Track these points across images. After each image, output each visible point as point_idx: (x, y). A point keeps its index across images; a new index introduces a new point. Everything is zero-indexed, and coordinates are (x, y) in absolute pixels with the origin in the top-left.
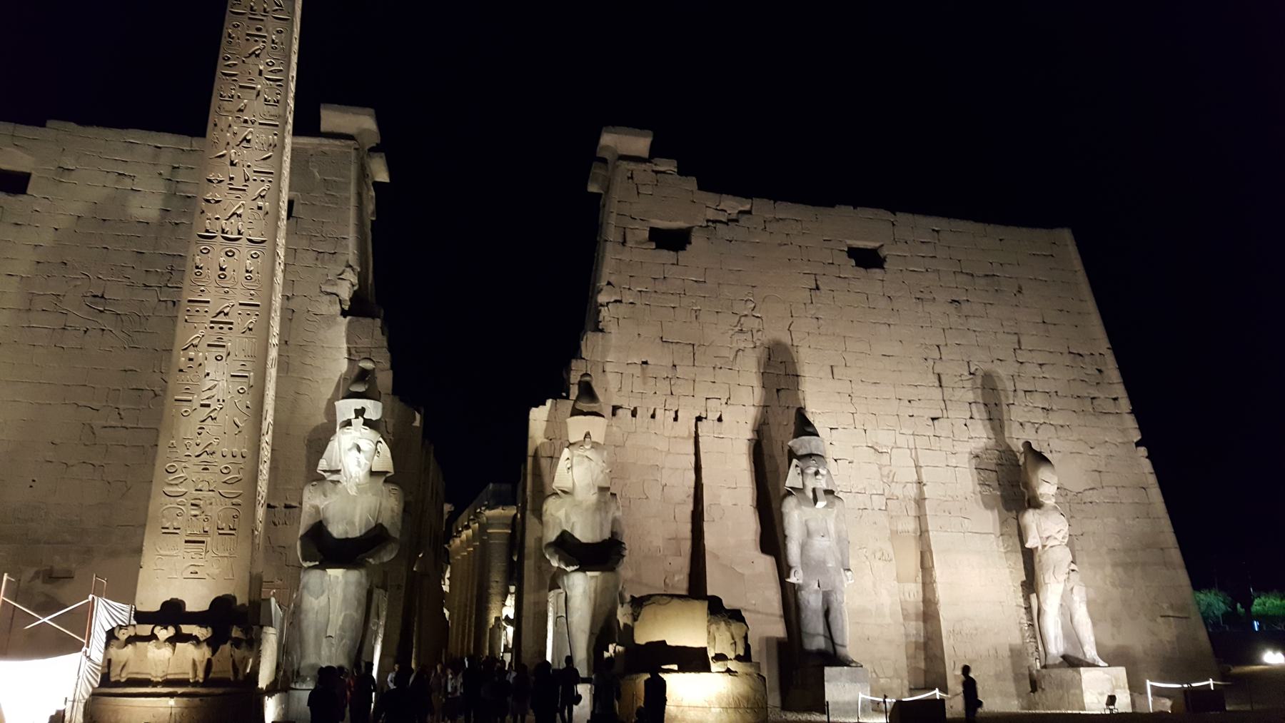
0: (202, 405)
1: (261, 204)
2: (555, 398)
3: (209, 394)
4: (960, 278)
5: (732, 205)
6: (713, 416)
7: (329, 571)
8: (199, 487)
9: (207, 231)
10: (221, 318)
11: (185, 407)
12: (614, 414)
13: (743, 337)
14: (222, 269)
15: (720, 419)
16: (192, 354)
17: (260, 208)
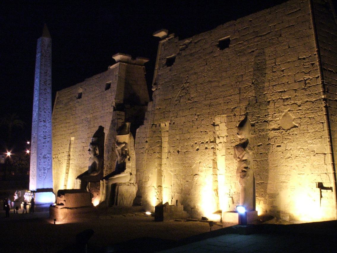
4: (256, 40)
5: (187, 41)
6: (172, 123)
12: (152, 127)
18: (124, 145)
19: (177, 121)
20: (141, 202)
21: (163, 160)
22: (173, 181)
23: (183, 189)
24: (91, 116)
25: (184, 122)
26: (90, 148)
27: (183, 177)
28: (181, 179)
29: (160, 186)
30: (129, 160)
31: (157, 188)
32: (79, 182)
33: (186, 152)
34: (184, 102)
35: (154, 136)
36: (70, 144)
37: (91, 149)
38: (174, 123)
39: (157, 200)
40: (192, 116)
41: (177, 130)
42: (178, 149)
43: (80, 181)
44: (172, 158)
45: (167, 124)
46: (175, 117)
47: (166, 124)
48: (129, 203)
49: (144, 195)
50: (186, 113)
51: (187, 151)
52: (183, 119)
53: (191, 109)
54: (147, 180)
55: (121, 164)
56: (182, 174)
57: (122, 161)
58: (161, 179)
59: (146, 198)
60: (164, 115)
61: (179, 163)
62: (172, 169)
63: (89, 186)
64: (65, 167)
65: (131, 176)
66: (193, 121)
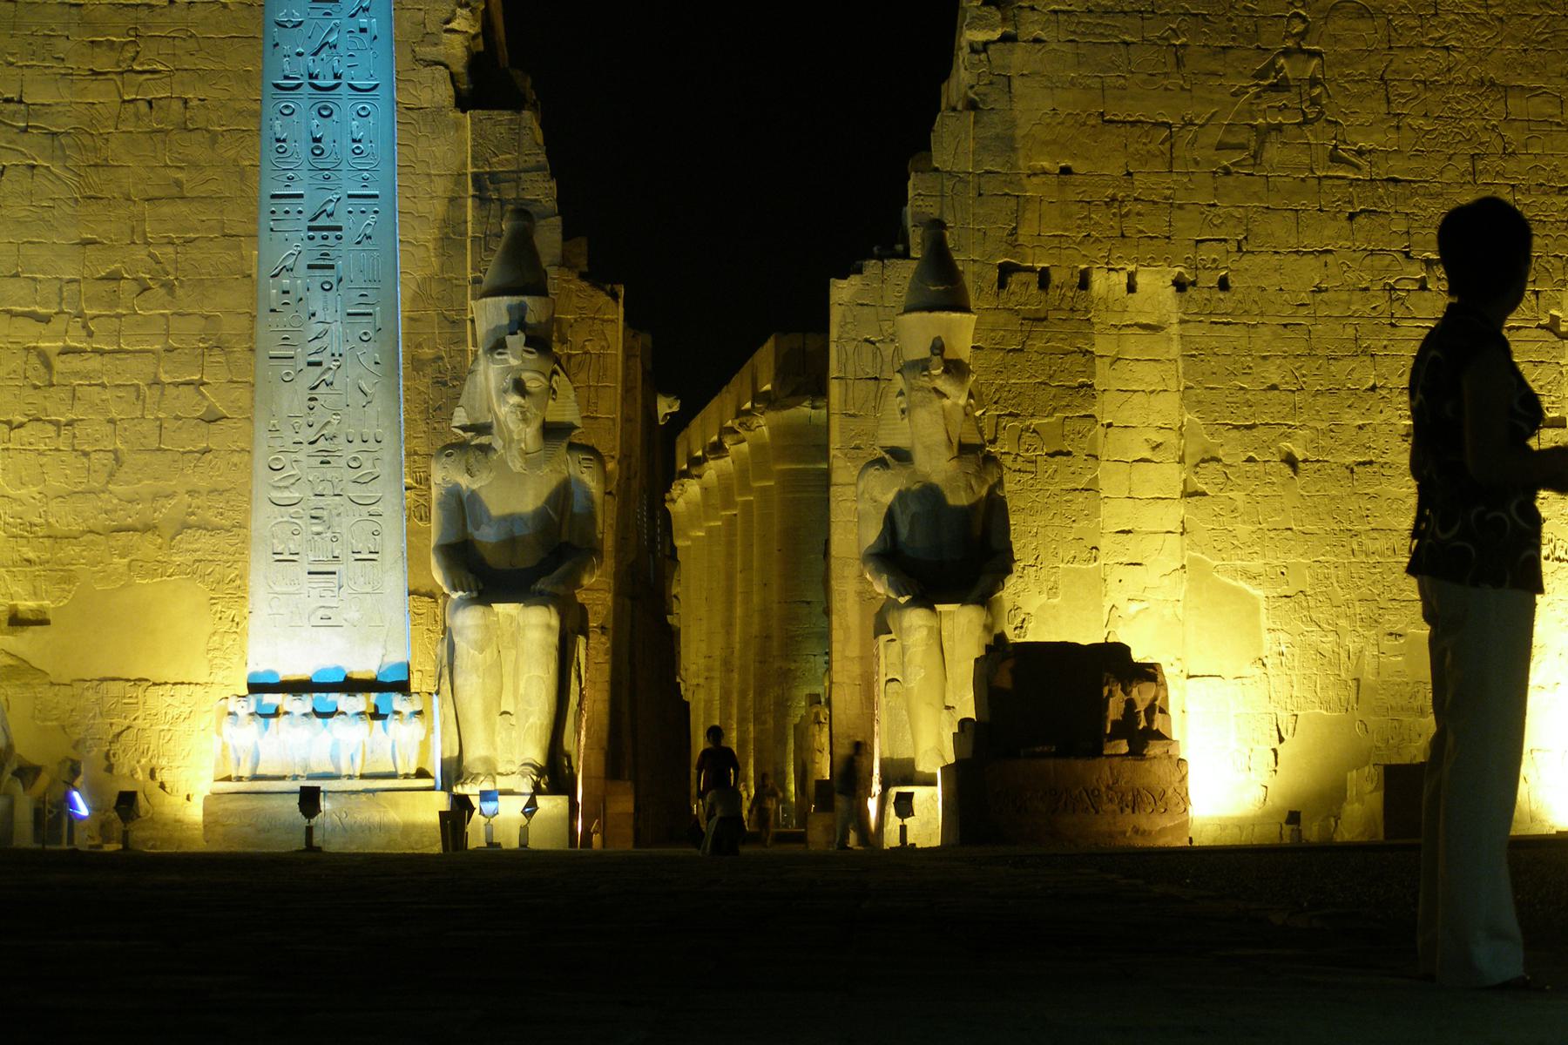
0: (310, 364)
1: (363, 21)
2: (881, 258)
3: (317, 344)
6: (1209, 279)
7: (500, 608)
8: (319, 490)
9: (287, 78)
10: (323, 221)
11: (285, 368)
12: (1002, 284)
13: (1281, 99)
14: (317, 140)
15: (1224, 285)
16: (286, 282)
17: (363, 30)
19: (1249, 272)
23: (1369, 677)
24: (102, 95)
25: (1320, 290)
26: (526, 376)
27: (1358, 608)
28: (1343, 622)
32: (549, 627)
33: (1359, 464)
34: (1300, 170)
35: (1039, 345)
37: (534, 383)
40: (1377, 262)
41: (1263, 329)
42: (1286, 445)
43: (555, 622)
45: (1155, 283)
46: (1233, 247)
47: (1139, 279)
50: (1330, 233)
51: (1371, 463)
52: (1310, 272)
53: (1361, 220)
55: (966, 513)
56: (1341, 595)
57: (984, 492)
60: (1124, 223)
61: (1310, 528)
62: (1256, 564)
66: (1393, 289)
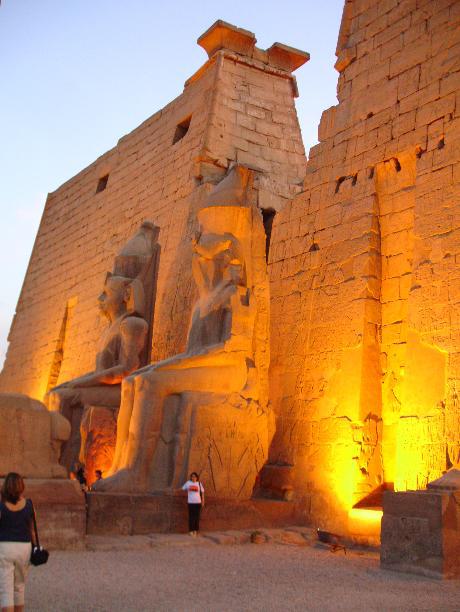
6: (433, 144)
18: (226, 246)
20: (289, 487)
21: (386, 311)
22: (447, 385)
29: (374, 418)
30: (246, 301)
31: (360, 424)
36: (65, 319)
38: (442, 145)
39: (361, 478)
44: (438, 284)
48: (236, 484)
49: (300, 453)
54: (316, 393)
58: (380, 389)
59: (312, 468)
63: (88, 420)
64: (46, 383)
65: (252, 370)
